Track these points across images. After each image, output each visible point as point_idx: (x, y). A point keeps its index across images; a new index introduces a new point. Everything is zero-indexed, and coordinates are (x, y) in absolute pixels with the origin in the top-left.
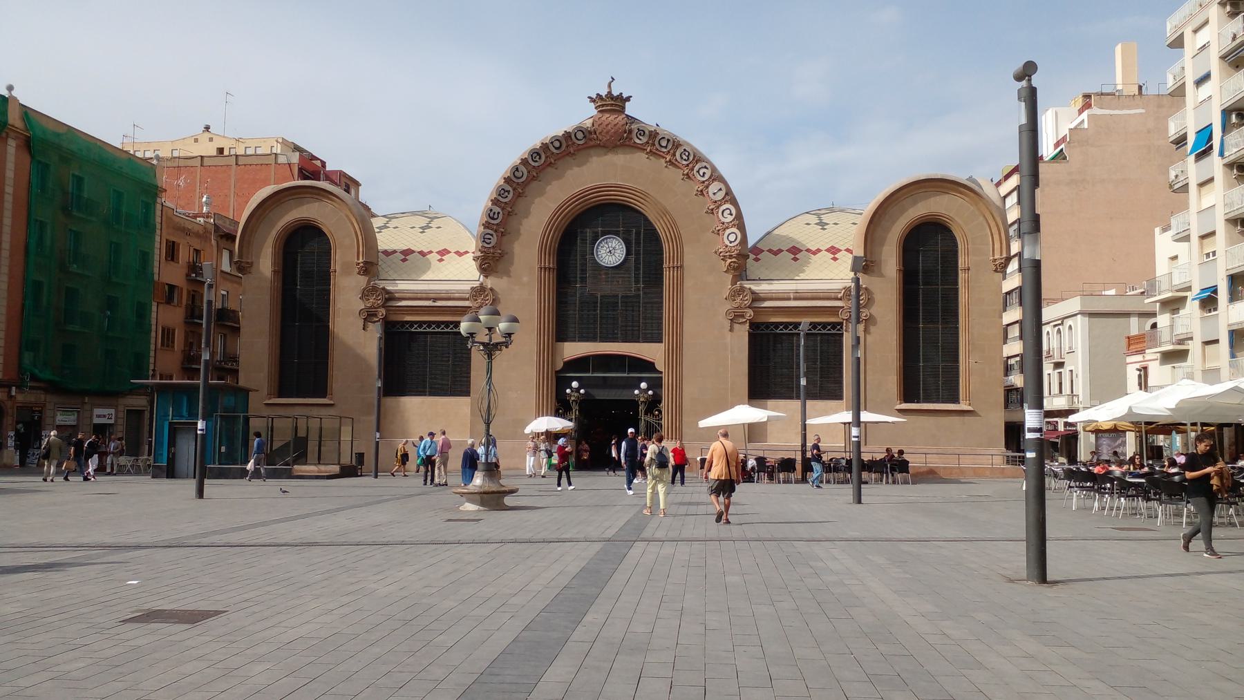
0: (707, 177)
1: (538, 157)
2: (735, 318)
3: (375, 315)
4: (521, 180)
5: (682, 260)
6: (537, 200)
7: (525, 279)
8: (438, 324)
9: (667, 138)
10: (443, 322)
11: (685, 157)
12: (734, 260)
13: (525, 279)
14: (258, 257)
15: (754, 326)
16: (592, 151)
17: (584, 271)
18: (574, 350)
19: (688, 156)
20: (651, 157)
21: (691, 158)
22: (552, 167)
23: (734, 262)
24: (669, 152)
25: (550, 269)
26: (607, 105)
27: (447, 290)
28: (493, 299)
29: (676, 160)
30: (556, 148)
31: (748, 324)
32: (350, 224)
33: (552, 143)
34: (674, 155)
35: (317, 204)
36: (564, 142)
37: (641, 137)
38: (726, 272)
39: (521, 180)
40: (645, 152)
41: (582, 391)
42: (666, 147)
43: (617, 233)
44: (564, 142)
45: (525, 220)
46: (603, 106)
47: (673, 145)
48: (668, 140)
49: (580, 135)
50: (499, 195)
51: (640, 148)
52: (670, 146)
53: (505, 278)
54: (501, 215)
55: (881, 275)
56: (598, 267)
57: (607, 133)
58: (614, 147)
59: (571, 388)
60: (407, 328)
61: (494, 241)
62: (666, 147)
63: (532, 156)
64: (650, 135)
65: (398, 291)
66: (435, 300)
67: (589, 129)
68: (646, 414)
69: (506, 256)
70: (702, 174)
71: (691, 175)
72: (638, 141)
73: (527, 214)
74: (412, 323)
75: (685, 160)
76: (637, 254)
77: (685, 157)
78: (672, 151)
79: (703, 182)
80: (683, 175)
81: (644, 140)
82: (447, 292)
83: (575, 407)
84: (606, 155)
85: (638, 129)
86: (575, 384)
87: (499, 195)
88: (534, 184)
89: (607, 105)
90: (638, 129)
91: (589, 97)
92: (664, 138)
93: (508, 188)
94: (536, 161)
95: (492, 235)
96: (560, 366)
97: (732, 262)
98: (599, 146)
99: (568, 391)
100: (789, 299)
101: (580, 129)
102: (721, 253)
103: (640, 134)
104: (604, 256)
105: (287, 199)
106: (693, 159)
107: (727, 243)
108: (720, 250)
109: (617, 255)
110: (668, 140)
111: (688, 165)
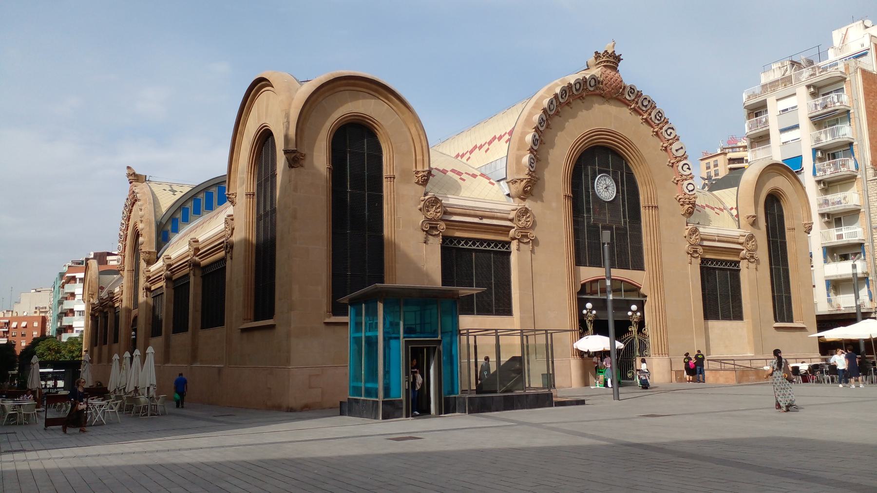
0: (672, 136)
2: (693, 253)
3: (436, 228)
5: (657, 203)
6: (559, 134)
7: (554, 205)
8: (482, 241)
9: (648, 99)
10: (485, 241)
11: (658, 117)
12: (691, 206)
13: (554, 205)
14: (312, 147)
15: (704, 261)
16: (595, 99)
17: (588, 202)
18: (589, 273)
19: (660, 117)
20: (632, 113)
21: (662, 119)
22: (569, 106)
23: (691, 207)
24: (647, 111)
25: (568, 196)
26: (611, 62)
27: (490, 209)
28: (533, 221)
29: (651, 118)
30: (577, 90)
32: (406, 129)
34: (650, 114)
35: (373, 101)
36: (582, 85)
37: (631, 95)
40: (629, 108)
41: (594, 312)
42: (646, 106)
43: (608, 172)
44: (582, 85)
45: (551, 150)
46: (608, 61)
47: (651, 106)
48: (649, 101)
49: (593, 83)
51: (626, 104)
52: (649, 107)
53: (539, 202)
55: (759, 229)
56: (597, 199)
57: (611, 85)
58: (609, 99)
60: (455, 245)
62: (646, 106)
63: (562, 93)
64: (637, 94)
65: (451, 206)
66: (482, 217)
67: (599, 79)
68: (638, 333)
69: (539, 181)
70: (669, 134)
71: (659, 133)
72: (628, 97)
73: (552, 146)
74: (459, 239)
75: (658, 120)
76: (623, 191)
77: (658, 117)
78: (649, 111)
79: (668, 140)
80: (653, 132)
81: (633, 97)
82: (491, 210)
83: (590, 328)
84: (603, 104)
85: (631, 87)
86: (589, 305)
88: (557, 118)
89: (611, 62)
90: (631, 87)
92: (646, 99)
98: (600, 95)
99: (585, 312)
100: (714, 241)
102: (680, 199)
103: (631, 92)
104: (602, 191)
105: (342, 89)
106: (663, 121)
107: (687, 192)
108: (680, 197)
109: (610, 191)
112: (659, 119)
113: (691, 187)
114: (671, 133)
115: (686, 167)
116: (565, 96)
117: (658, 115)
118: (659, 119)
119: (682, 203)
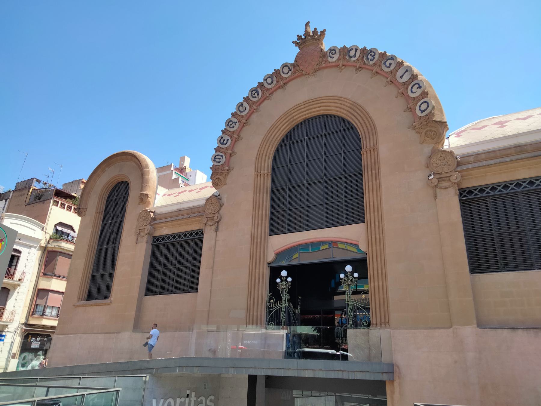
0: (392, 67)
1: (256, 94)
4: (243, 114)
19: (373, 56)
33: (265, 80)
39: (243, 114)
49: (286, 70)
50: (228, 125)
54: (229, 142)
58: (313, 73)
59: (281, 278)
61: (223, 160)
63: (252, 94)
77: (370, 57)
81: (336, 57)
86: (284, 273)
87: (228, 125)
91: (293, 42)
93: (234, 120)
94: (255, 97)
95: (222, 156)
96: (271, 257)
99: (278, 280)
101: (285, 65)
110: (356, 50)
112: (372, 58)
113: (423, 107)
114: (390, 64)
115: (414, 89)
116: (258, 95)
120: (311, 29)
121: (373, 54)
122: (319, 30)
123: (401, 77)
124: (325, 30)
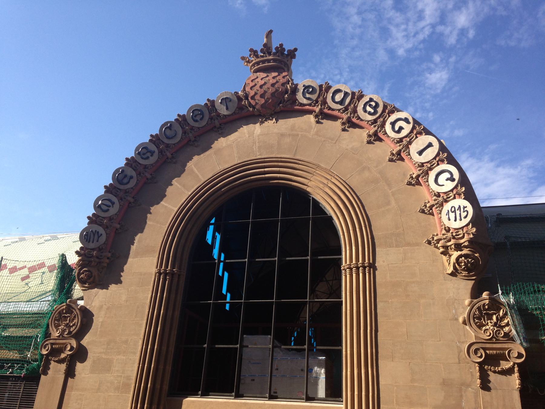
12: (465, 251)
21: (380, 110)
23: (466, 256)
31: (516, 375)
38: (453, 274)
70: (397, 128)
75: (370, 113)
79: (401, 140)
89: (269, 61)
97: (461, 256)
111: (375, 121)
112: (372, 111)
117: (370, 106)
118: (372, 111)
119: (442, 250)
120: (275, 44)
121: (373, 104)
122: (288, 47)
123: (420, 153)
124: (296, 50)
